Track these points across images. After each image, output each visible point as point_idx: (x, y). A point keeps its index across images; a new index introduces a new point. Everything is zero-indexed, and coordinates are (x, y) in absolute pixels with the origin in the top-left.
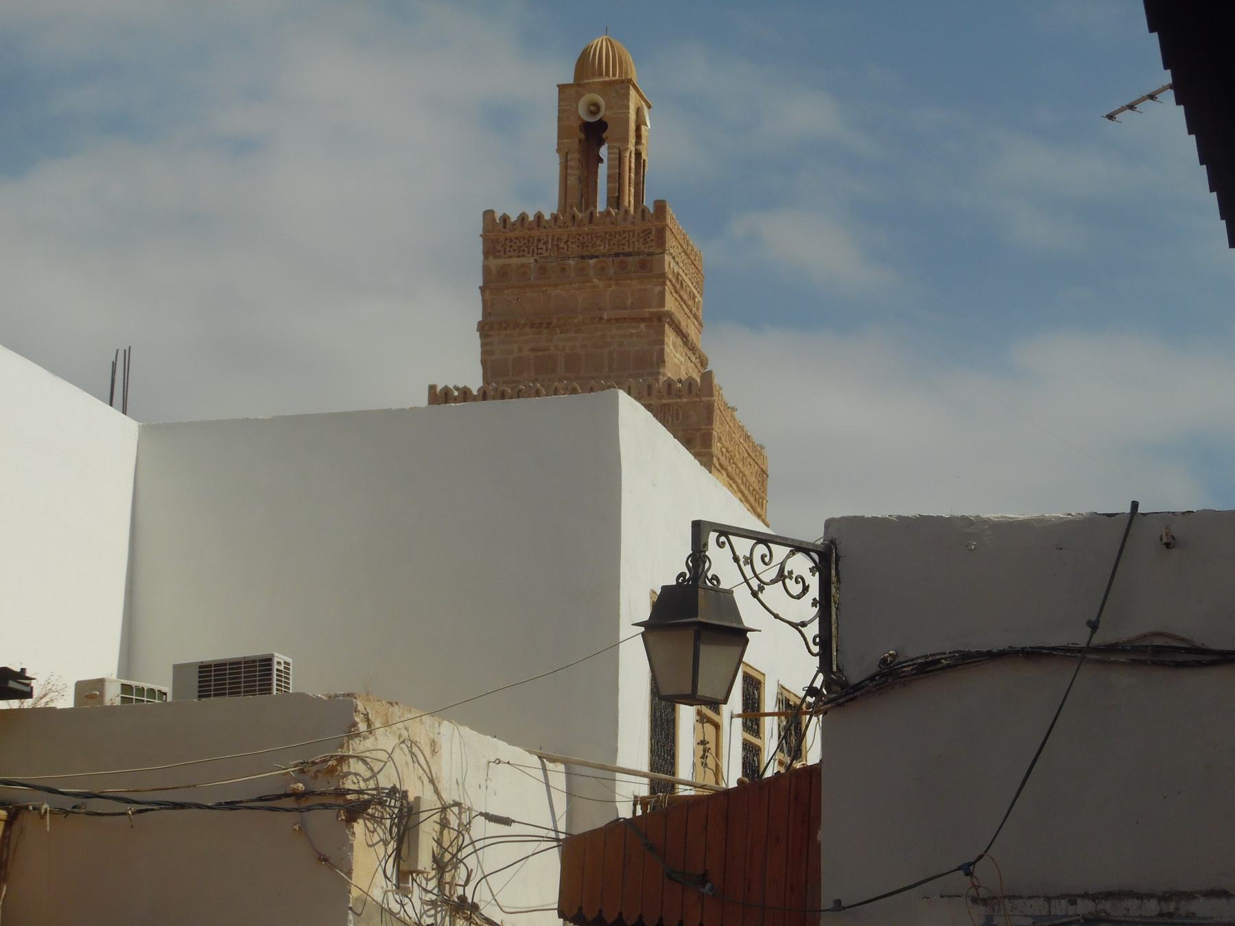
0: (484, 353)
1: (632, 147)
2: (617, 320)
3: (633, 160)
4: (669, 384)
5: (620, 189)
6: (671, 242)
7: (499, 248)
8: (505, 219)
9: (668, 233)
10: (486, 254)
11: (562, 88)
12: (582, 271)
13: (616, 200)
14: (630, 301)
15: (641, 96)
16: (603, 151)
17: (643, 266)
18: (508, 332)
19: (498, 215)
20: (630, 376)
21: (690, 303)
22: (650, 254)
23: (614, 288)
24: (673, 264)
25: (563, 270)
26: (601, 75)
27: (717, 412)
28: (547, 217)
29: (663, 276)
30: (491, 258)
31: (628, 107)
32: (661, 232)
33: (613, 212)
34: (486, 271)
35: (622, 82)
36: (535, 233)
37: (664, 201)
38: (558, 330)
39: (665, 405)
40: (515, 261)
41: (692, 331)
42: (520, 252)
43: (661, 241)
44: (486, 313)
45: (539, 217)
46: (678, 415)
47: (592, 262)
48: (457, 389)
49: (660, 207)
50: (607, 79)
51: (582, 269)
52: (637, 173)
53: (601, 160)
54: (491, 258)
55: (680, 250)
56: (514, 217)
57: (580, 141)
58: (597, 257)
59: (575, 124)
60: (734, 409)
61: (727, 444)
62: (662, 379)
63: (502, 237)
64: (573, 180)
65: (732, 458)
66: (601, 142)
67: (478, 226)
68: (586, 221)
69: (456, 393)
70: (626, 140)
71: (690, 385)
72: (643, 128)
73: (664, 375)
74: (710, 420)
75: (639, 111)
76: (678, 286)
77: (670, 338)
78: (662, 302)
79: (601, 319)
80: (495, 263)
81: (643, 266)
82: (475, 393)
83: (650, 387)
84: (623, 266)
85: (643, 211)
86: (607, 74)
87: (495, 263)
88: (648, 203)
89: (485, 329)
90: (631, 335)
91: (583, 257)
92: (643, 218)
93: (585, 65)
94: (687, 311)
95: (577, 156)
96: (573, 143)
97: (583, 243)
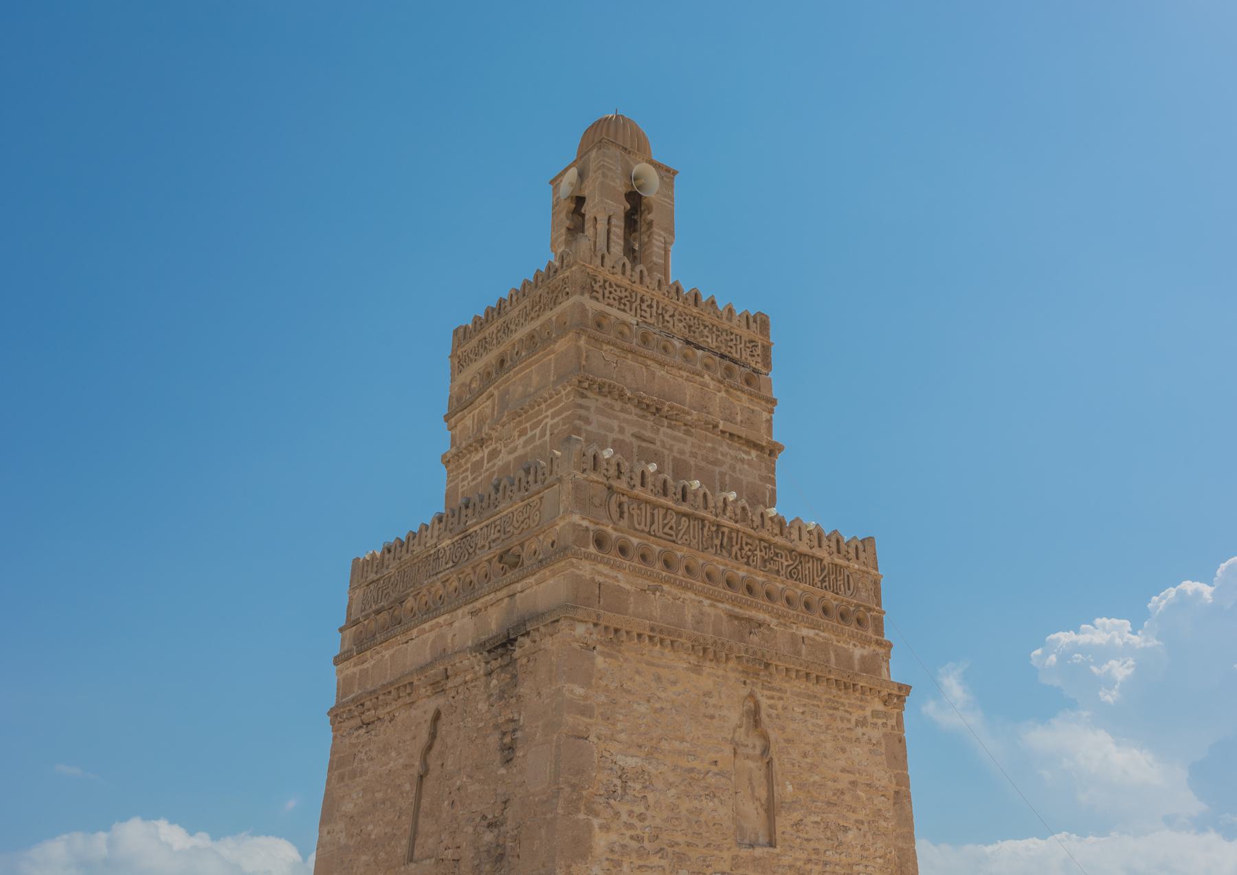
14: (739, 418)
18: (609, 400)
23: (723, 394)
38: (666, 422)
47: (700, 353)
84: (729, 372)
97: (690, 326)
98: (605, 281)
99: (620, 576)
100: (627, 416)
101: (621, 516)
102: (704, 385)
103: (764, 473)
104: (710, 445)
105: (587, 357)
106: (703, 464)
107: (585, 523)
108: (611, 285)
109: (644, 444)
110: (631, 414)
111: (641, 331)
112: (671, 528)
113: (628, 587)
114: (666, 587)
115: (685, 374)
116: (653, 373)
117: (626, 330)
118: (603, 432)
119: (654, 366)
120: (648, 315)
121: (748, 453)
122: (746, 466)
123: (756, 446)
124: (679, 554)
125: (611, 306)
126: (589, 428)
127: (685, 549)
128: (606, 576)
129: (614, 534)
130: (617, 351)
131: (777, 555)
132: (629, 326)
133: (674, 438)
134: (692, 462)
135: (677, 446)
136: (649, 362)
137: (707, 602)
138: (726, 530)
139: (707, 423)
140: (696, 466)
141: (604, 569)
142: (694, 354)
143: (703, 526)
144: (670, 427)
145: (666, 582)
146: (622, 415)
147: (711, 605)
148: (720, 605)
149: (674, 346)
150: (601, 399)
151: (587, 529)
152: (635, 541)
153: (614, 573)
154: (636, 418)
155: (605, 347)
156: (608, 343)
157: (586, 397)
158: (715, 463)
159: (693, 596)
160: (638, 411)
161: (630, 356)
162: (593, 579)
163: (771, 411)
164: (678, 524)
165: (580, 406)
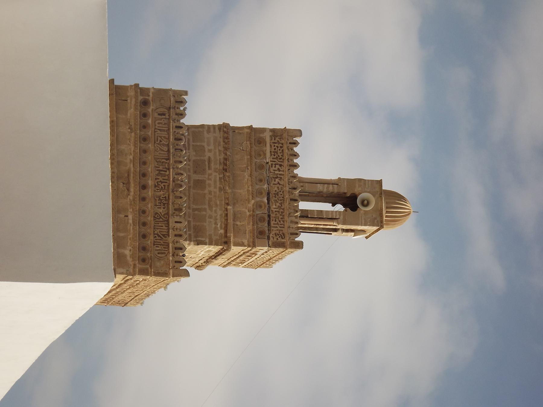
0: (209, 126)
1: (340, 227)
2: (227, 215)
3: (331, 227)
4: (182, 249)
5: (313, 218)
6: (276, 251)
7: (277, 139)
8: (296, 144)
9: (281, 250)
10: (273, 131)
11: (380, 182)
12: (260, 193)
13: (306, 215)
14: (238, 223)
15: (373, 233)
16: (339, 208)
17: (261, 233)
18: (222, 143)
19: (298, 139)
20: (189, 222)
21: (238, 261)
22: (269, 238)
23: (248, 214)
24: (262, 252)
25: (261, 181)
26: (387, 208)
27: (162, 279)
28: (296, 171)
29: (254, 246)
30: (271, 134)
31: (365, 225)
32: (282, 245)
33: (298, 214)
34: (262, 130)
35: (382, 222)
36: (286, 163)
37: (302, 248)
38: (222, 176)
39: (168, 245)
41: (221, 260)
42: (274, 153)
43: (277, 245)
44: (234, 129)
45: (296, 166)
46: (162, 253)
47: (265, 200)
48: (185, 109)
49: (299, 245)
50: (384, 212)
51: (261, 193)
52: (324, 229)
53: (333, 205)
54: (271, 134)
55: (272, 256)
56: (295, 149)
57: (345, 193)
58: (268, 203)
59: (357, 190)
60: (165, 288)
61: (142, 283)
62: (186, 244)
63: (284, 142)
64: (320, 188)
65: (133, 286)
66: (344, 206)
67: (291, 126)
68: (292, 197)
69: (182, 108)
70: (344, 223)
71: (181, 262)
72: (353, 234)
73: (189, 244)
74: (157, 274)
75: (363, 231)
76: (248, 254)
77: (214, 249)
78: (236, 244)
79: (228, 204)
80: (267, 136)
81: (261, 233)
82: (182, 121)
83: (180, 236)
84: (262, 220)
85: (297, 234)
86: (387, 212)
87: (267, 136)
88: (302, 237)
89: (224, 128)
90: (216, 224)
91: (268, 194)
92: (292, 234)
93: (394, 198)
94: (232, 259)
95: (336, 191)
96: (344, 189)
97: (277, 194)
98: (282, 144)
99: (132, 109)
100: (218, 154)
101: (159, 114)
102: (249, 202)
103: (214, 238)
104: (218, 203)
105: (240, 133)
106: (207, 198)
109: (207, 163)
110: (219, 156)
111: (264, 164)
112: (161, 141)
113: (129, 115)
114: (133, 134)
115: (250, 189)
118: (206, 140)
120: (274, 168)
121: (221, 228)
122: (214, 226)
123: (226, 232)
124: (150, 145)
126: (205, 133)
128: (131, 103)
129: (150, 110)
130: (248, 149)
133: (215, 182)
134: (206, 191)
135: (212, 182)
137: (131, 157)
138: (167, 173)
139: (228, 199)
140: (205, 194)
142: (264, 197)
143: (167, 159)
144: (220, 178)
145: (135, 134)
146: (217, 151)
147: (131, 160)
148: (132, 165)
150: (221, 140)
151: (149, 96)
152: (150, 121)
153: (133, 107)
155: (248, 143)
156: (251, 144)
157: (220, 131)
158: (210, 207)
159: (132, 150)
160: (222, 160)
161: (249, 157)
162: (128, 97)
164: (164, 145)
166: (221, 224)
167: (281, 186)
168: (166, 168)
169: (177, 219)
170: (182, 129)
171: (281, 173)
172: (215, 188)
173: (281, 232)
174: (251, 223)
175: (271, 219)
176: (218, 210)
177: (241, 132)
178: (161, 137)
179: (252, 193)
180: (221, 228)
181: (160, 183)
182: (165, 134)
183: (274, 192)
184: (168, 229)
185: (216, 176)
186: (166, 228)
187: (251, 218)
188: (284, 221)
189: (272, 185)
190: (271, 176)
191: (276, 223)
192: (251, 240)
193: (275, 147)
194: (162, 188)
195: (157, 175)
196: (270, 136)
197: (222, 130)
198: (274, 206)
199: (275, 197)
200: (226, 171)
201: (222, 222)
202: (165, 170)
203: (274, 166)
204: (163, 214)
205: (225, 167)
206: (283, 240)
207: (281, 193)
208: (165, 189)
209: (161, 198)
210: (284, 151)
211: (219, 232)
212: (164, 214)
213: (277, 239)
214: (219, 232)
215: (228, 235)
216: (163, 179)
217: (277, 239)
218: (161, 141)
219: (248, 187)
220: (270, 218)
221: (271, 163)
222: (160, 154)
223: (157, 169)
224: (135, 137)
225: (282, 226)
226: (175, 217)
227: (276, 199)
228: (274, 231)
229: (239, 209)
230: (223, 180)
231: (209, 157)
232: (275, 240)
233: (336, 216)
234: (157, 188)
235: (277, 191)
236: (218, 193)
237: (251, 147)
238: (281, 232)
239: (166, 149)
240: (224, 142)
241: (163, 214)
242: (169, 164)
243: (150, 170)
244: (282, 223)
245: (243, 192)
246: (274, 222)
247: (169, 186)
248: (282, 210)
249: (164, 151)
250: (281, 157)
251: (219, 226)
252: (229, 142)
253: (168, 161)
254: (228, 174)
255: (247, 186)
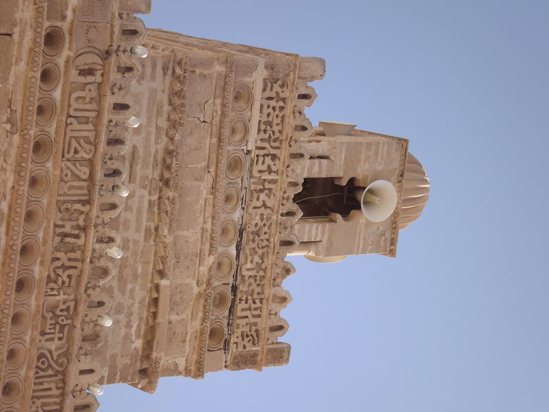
2: (156, 301)
7: (276, 88)
18: (166, 108)
22: (227, 343)
23: (196, 290)
38: (155, 198)
40: (256, 116)
47: (233, 251)
90: (128, 325)
98: (284, 100)
99: (23, 65)
102: (201, 256)
104: (140, 271)
105: (205, 76)
107: (69, 14)
108: (282, 108)
110: (157, 143)
112: (76, 152)
113: (12, 79)
114: (16, 139)
115: (208, 226)
116: (199, 179)
117: (238, 137)
119: (209, 179)
120: (261, 167)
121: (138, 336)
122: (123, 331)
123: (149, 344)
124: (49, 165)
125: (261, 111)
127: (58, 172)
128: (20, 44)
129: (61, 61)
131: (63, 327)
132: (244, 139)
133: (139, 213)
135: (131, 216)
136: (212, 170)
138: (81, 242)
139: (163, 260)
141: (27, 43)
143: (84, 203)
145: (23, 137)
146: (153, 129)
149: (234, 210)
150: (165, 98)
151: (64, 18)
152: (57, 94)
153: (25, 56)
154: (153, 151)
155: (218, 101)
156: (224, 105)
157: (165, 74)
159: (10, 184)
160: (161, 154)
161: (215, 140)
162: (14, 25)
163: (188, 372)
165: (154, 67)
166: (139, 325)
167: (268, 211)
168: (78, 227)
169: (86, 363)
170: (127, 112)
171: (273, 177)
172: (137, 230)
173: (254, 328)
174: (201, 315)
175: (239, 296)
176: (138, 288)
177: (206, 72)
178: (77, 139)
179: (212, 238)
180: (138, 336)
181: (60, 272)
182: (87, 130)
183: (253, 229)
184: (63, 395)
185: (142, 197)
186: (58, 392)
187: (202, 301)
188: (261, 300)
189: (250, 210)
190: (253, 187)
191: (247, 306)
192: (195, 357)
193: (271, 110)
194: (63, 283)
195: (57, 249)
196: (265, 80)
197: (170, 72)
198: (249, 265)
199: (253, 241)
200: (167, 183)
201: (141, 319)
202: (76, 232)
203: (261, 159)
204: (55, 355)
205: (167, 175)
206: (255, 349)
207: (266, 229)
208: (69, 286)
209: (58, 312)
210: (287, 120)
211: (133, 346)
212: (59, 356)
213: (244, 347)
214: (133, 346)
215: (154, 355)
216: (69, 260)
217: (244, 347)
218: (76, 152)
219: (205, 222)
220: (235, 295)
221: (258, 152)
222: (71, 188)
223: (59, 230)
224: (22, 148)
225: (258, 312)
226: (82, 358)
227: (255, 245)
228: (242, 326)
229: (179, 282)
230: (156, 209)
231: (134, 147)
232: (240, 349)
233: (315, 238)
234: (52, 285)
235: (260, 224)
236: (142, 240)
237: (223, 115)
238: (254, 328)
239: (84, 172)
240: (170, 104)
241: (55, 355)
242: (87, 214)
243: (41, 235)
244: (258, 305)
245: (191, 236)
246: (243, 305)
247: (79, 276)
248: (261, 273)
249: (80, 179)
250: (277, 135)
251: (133, 331)
252: (183, 105)
253: (86, 209)
254: (171, 194)
255: (201, 219)
